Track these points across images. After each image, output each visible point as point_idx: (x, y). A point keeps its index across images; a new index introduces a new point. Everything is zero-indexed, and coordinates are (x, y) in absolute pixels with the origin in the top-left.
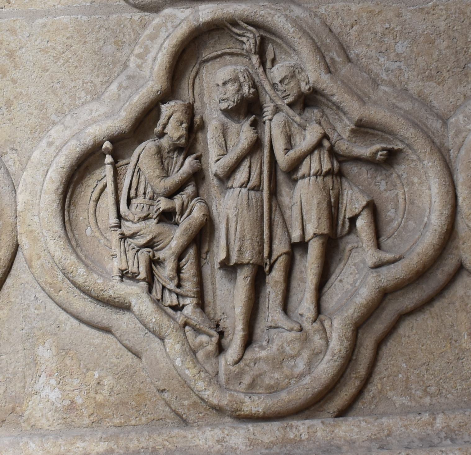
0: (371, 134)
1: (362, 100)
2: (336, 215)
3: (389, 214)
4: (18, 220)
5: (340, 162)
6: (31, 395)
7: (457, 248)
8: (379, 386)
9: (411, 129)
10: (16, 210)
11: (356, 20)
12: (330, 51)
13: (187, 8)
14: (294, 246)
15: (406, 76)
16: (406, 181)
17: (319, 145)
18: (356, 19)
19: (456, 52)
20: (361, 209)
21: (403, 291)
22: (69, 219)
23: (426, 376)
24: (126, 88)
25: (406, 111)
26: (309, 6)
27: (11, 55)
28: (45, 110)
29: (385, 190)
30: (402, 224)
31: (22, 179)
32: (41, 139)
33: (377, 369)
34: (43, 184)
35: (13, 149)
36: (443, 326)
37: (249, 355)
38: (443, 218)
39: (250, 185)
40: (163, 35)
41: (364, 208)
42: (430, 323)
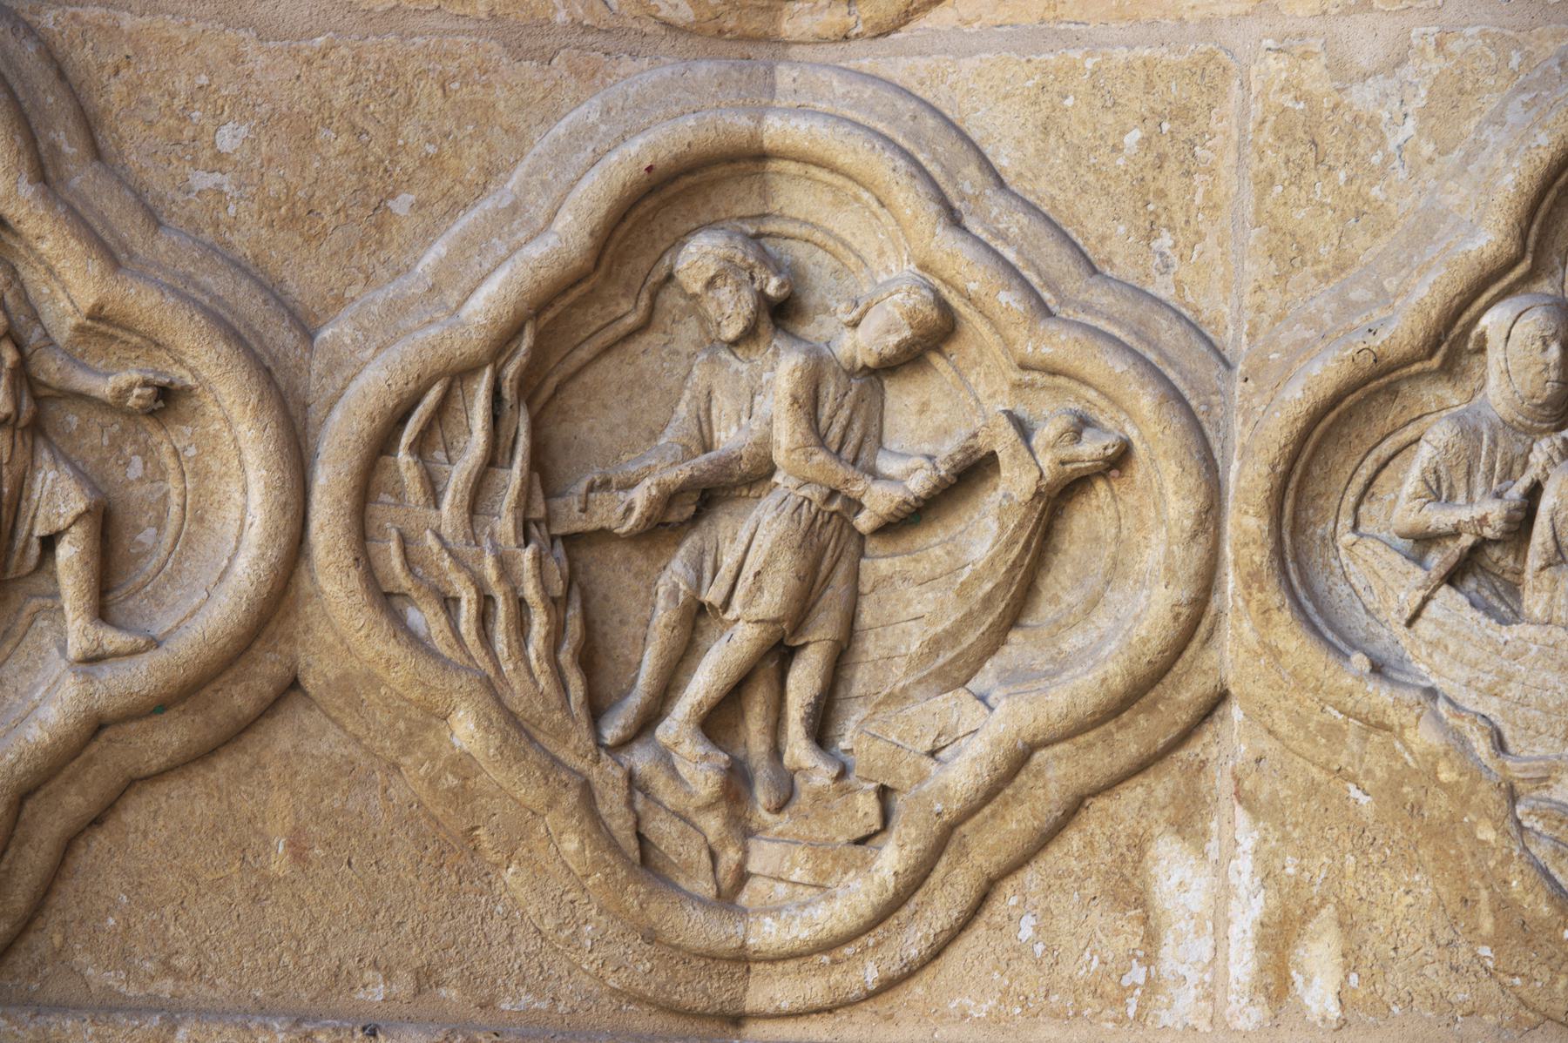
0: (122, 342)
1: (113, 256)
2: (9, 526)
3: (140, 537)
5: (37, 400)
7: (290, 639)
8: (57, 939)
9: (221, 343)
11: (128, 57)
15: (232, 211)
16: (191, 465)
18: (130, 53)
19: (364, 168)
20: (70, 520)
21: (145, 723)
23: (172, 928)
29: (140, 480)
30: (169, 565)
33: (54, 900)
36: (231, 821)
38: (263, 565)
41: (78, 519)
42: (201, 805)
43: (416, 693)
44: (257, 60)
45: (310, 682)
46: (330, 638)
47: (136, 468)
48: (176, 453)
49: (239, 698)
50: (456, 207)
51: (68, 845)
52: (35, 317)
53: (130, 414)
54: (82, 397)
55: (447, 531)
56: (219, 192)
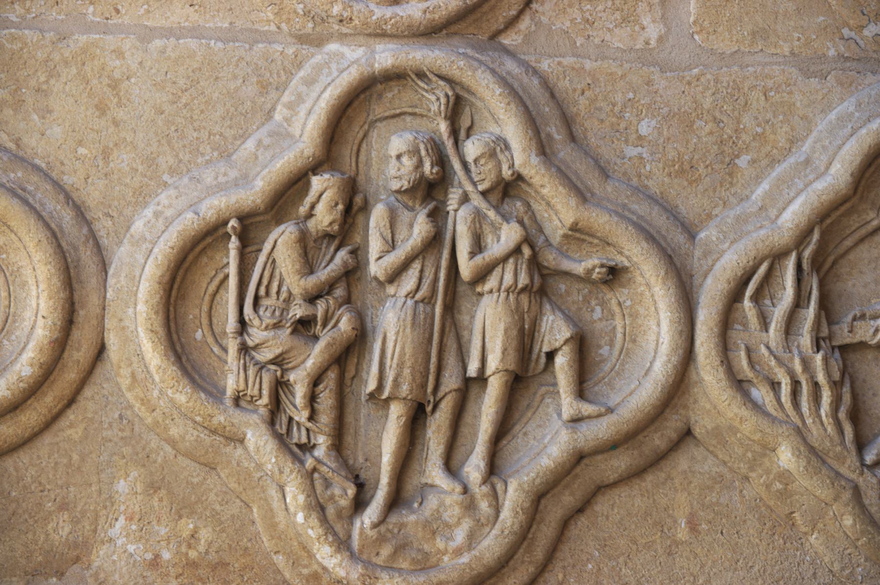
0: (589, 243)
1: (582, 195)
2: (529, 346)
3: (601, 351)
4: (106, 312)
5: (542, 276)
6: (103, 543)
7: (686, 407)
8: (560, 576)
9: (644, 242)
10: (105, 297)
11: (589, 84)
12: (547, 125)
13: (360, 46)
14: (468, 382)
15: (648, 168)
16: (628, 310)
17: (517, 251)
18: (590, 82)
19: (721, 142)
20: (562, 342)
21: (605, 455)
22: (175, 318)
23: (623, 570)
24: (267, 148)
25: (640, 217)
26: (526, 58)
27: (114, 85)
28: (155, 166)
29: (600, 319)
30: (617, 367)
31: (116, 257)
32: (146, 205)
33: (559, 554)
34: (144, 267)
35: (108, 215)
36: (655, 509)
37: (393, 519)
38: (670, 366)
39: (419, 296)
40: (324, 80)
41: (566, 342)
42: (638, 501)
43: (757, 437)
44: (660, 83)
45: (697, 431)
46: (708, 406)
47: (598, 313)
48: (620, 304)
49: (658, 440)
50: (774, 162)
51: (565, 524)
52: (541, 230)
53: (593, 283)
54: (567, 274)
55: (773, 344)
56: (641, 158)
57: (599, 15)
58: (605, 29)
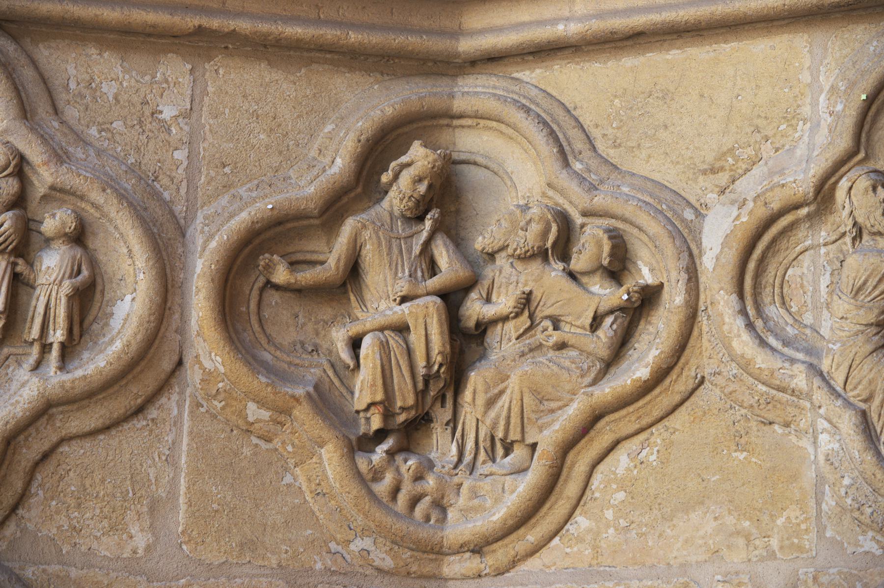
26: (10, 565)
57: (87, 522)
58: (92, 537)
